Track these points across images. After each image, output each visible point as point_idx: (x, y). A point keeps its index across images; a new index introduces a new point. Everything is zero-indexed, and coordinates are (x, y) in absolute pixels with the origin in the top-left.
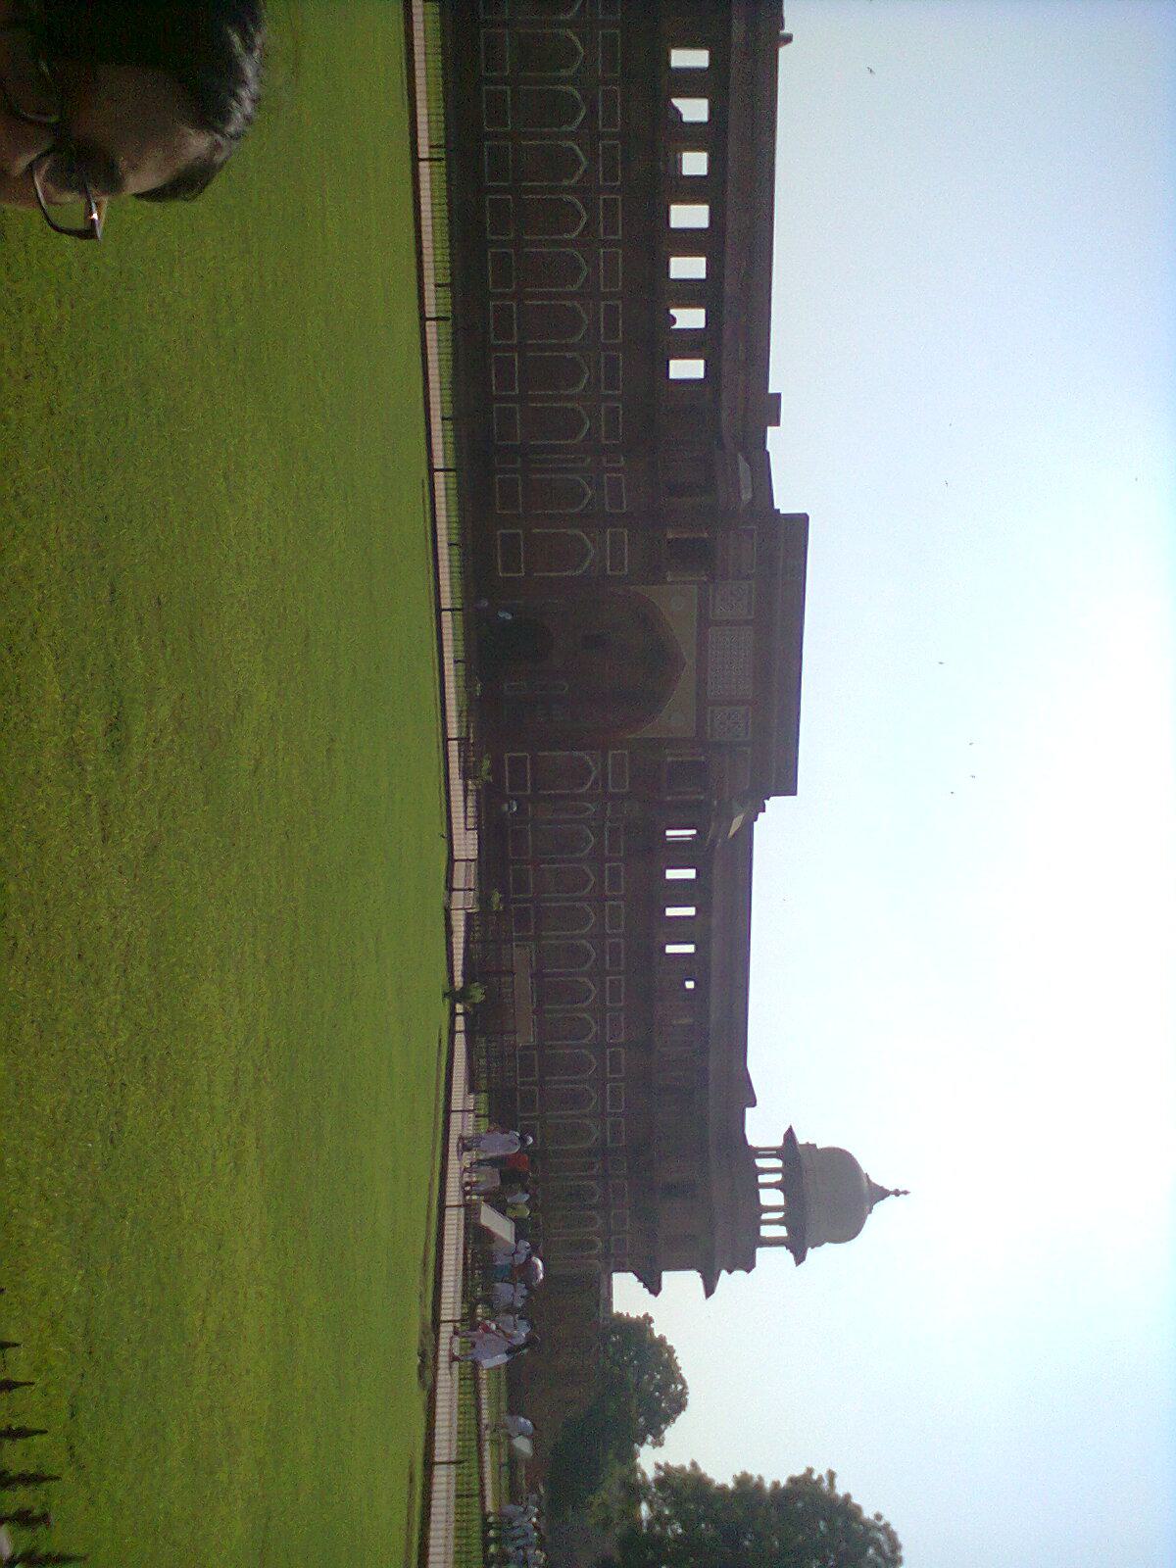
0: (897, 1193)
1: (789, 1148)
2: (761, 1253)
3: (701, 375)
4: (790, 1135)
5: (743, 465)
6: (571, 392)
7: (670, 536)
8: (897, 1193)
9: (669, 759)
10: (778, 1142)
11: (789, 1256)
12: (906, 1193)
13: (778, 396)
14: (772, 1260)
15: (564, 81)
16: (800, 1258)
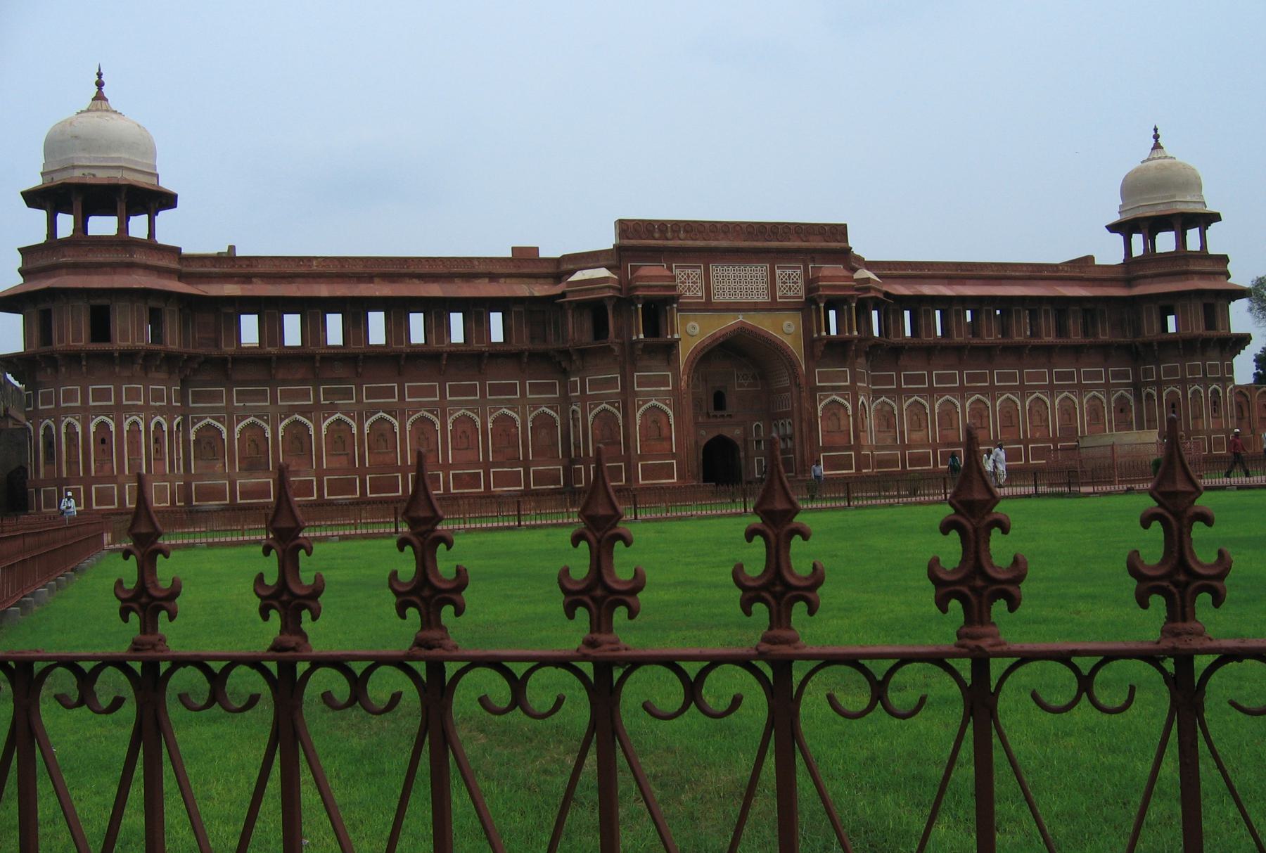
0: (1156, 137)
1: (1124, 228)
2: (1212, 250)
3: (500, 315)
4: (1113, 228)
5: (579, 276)
6: (519, 424)
7: (642, 336)
8: (1156, 137)
9: (824, 333)
10: (1118, 239)
11: (1213, 225)
12: (1156, 130)
13: (513, 249)
14: (1217, 240)
15: (275, 434)
16: (1216, 217)
